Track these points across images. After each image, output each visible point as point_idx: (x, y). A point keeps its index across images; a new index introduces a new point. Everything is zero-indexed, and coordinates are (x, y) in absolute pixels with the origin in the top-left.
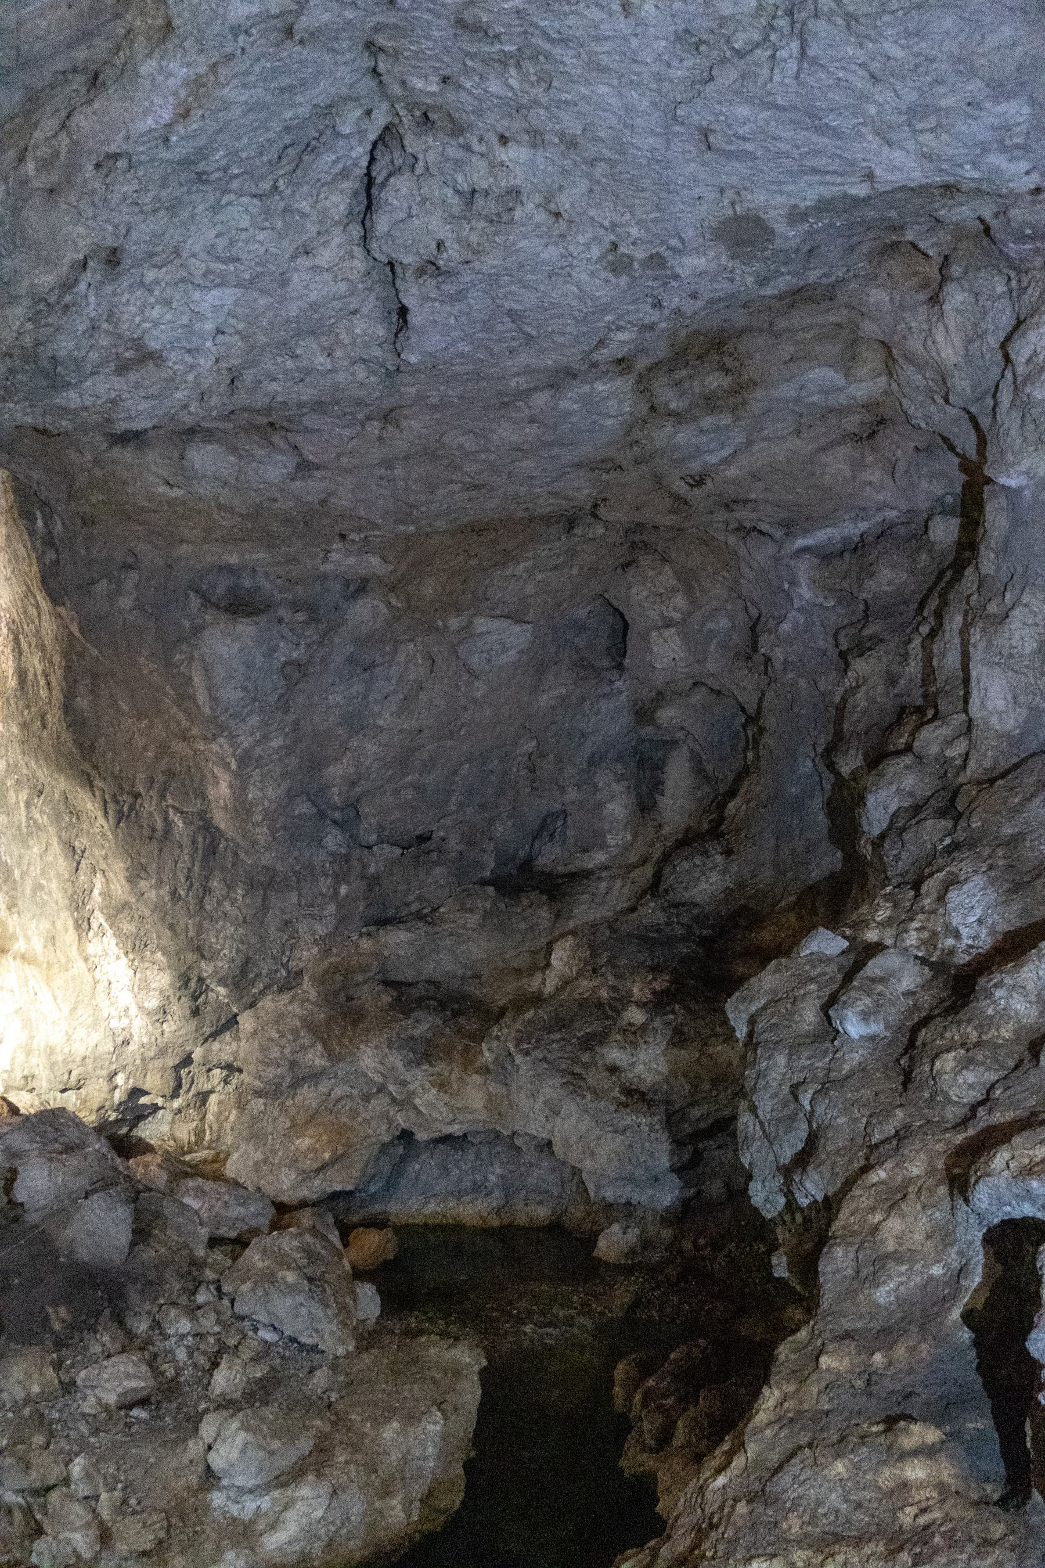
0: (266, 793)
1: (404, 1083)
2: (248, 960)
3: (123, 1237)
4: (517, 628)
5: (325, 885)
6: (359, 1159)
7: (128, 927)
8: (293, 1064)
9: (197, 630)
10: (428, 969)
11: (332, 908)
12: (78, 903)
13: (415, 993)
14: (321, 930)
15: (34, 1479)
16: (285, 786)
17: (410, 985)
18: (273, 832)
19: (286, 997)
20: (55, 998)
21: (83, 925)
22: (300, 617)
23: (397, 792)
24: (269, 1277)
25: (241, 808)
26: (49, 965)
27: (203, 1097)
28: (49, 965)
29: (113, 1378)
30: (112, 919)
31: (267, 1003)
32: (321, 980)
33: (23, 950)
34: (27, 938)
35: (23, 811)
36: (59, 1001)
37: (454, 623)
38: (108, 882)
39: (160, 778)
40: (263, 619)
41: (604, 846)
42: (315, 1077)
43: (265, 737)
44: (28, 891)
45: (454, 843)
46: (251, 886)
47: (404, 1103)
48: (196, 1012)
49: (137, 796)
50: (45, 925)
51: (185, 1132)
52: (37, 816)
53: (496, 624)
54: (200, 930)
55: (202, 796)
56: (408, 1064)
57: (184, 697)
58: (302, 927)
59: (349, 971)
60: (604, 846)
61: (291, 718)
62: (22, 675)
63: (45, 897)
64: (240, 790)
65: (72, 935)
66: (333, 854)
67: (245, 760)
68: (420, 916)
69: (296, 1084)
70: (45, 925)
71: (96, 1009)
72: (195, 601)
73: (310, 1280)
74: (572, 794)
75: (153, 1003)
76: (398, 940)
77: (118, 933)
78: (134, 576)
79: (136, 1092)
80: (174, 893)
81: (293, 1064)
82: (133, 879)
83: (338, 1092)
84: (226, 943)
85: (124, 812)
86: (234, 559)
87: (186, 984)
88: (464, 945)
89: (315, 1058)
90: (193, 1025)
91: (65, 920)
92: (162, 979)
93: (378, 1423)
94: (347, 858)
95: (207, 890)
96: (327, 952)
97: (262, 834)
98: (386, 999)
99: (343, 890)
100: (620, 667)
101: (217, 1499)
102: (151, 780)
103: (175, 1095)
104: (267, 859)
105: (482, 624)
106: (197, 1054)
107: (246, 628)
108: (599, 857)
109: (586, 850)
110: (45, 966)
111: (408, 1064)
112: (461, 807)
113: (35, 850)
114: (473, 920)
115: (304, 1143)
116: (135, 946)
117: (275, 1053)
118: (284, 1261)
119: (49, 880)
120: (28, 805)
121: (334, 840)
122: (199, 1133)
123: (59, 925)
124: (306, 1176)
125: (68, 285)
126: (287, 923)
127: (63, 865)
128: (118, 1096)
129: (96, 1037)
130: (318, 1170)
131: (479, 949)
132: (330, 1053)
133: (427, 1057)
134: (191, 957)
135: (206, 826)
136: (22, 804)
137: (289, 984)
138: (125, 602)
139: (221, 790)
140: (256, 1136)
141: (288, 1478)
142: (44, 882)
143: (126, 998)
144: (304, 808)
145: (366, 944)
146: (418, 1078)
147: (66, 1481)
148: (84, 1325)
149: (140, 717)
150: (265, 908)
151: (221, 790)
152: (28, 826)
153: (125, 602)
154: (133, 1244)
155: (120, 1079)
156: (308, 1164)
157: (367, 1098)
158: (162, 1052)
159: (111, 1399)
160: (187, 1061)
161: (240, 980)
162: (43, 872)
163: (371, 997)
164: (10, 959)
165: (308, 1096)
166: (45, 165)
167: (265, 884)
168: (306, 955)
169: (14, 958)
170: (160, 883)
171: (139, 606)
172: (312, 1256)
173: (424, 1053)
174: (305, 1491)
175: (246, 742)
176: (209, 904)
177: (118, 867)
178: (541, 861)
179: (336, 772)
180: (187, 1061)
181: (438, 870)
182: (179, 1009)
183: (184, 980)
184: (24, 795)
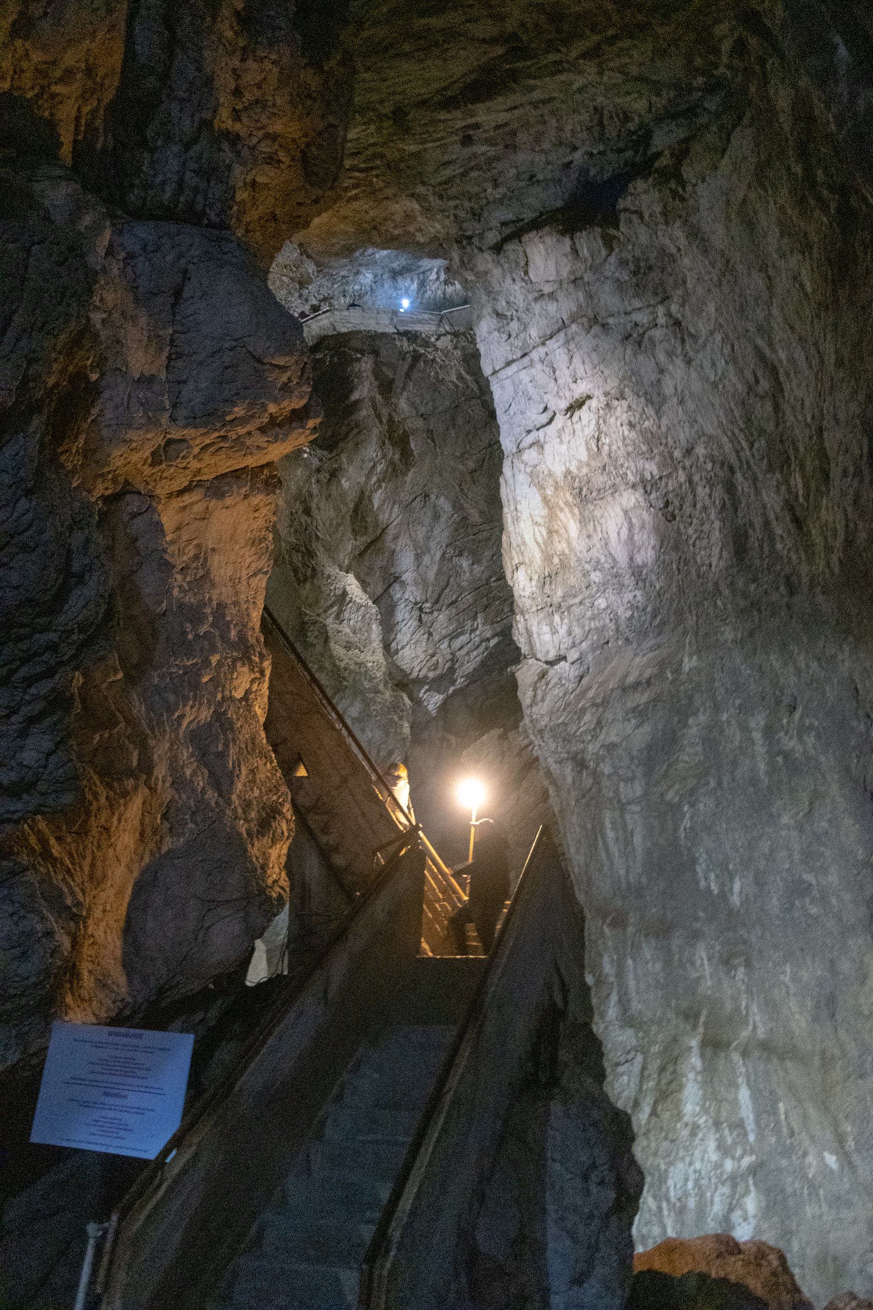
20: (841, 1139)
26: (827, 1063)
28: (827, 1063)
33: (761, 1033)
34: (772, 1008)
35: (760, 748)
36: (851, 1144)
44: (774, 903)
50: (812, 971)
52: (790, 743)
62: (739, 543)
63: (814, 910)
70: (812, 971)
110: (817, 1061)
113: (785, 820)
119: (824, 870)
120: (769, 732)
123: (845, 966)
136: (757, 736)
142: (809, 877)
152: (772, 770)
162: (808, 856)
164: (736, 1057)
169: (745, 1054)
184: (758, 722)
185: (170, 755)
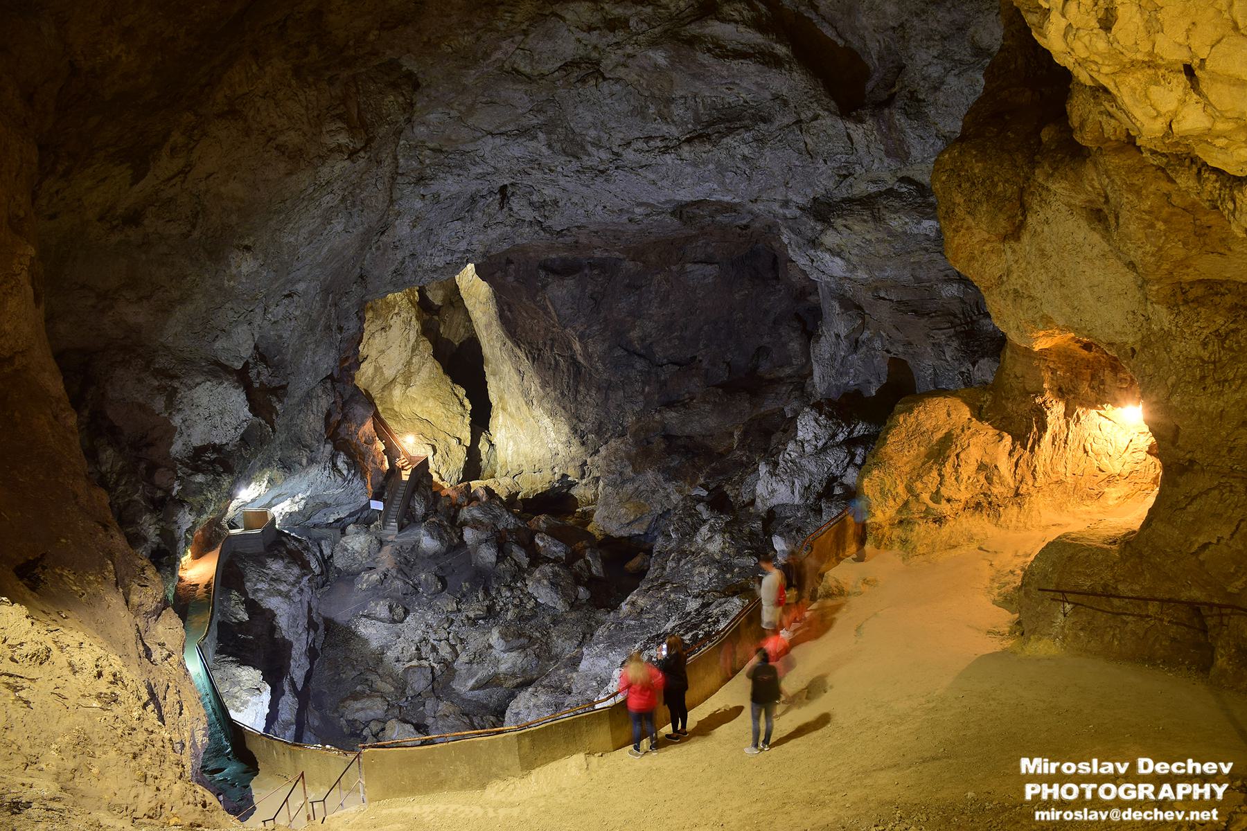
0: (597, 348)
1: (664, 489)
2: (601, 423)
3: (494, 559)
4: (710, 267)
5: (638, 386)
6: (648, 520)
7: (549, 406)
8: (621, 474)
9: (544, 287)
10: (687, 431)
11: (641, 398)
12: (525, 393)
13: (679, 442)
14: (637, 409)
15: (437, 637)
16: (606, 345)
17: (679, 437)
18: (604, 365)
19: (620, 441)
21: (529, 403)
22: (596, 272)
23: (670, 341)
24: (539, 581)
25: (588, 356)
27: (597, 479)
29: (474, 609)
30: (540, 402)
31: (612, 443)
32: (634, 435)
37: (674, 268)
38: (535, 387)
39: (549, 342)
40: (577, 276)
41: (791, 364)
42: (633, 480)
43: (590, 326)
45: (705, 364)
46: (599, 389)
47: (668, 497)
48: (583, 444)
49: (540, 350)
51: (589, 493)
53: (697, 266)
54: (577, 409)
55: (571, 349)
56: (666, 480)
57: (547, 313)
58: (627, 407)
59: (647, 431)
60: (791, 364)
61: (602, 315)
64: (585, 347)
65: (525, 408)
66: (641, 371)
67: (581, 338)
68: (684, 405)
69: (624, 482)
71: (542, 440)
72: (542, 274)
73: (552, 584)
74: (766, 339)
75: (564, 439)
76: (671, 416)
77: (544, 408)
78: (512, 266)
79: (564, 476)
80: (562, 393)
81: (621, 474)
82: (543, 387)
83: (642, 488)
84: (590, 415)
85: (536, 357)
86: (554, 256)
87: (576, 431)
88: (702, 421)
89: (629, 471)
90: (583, 449)
91: (522, 401)
92: (566, 429)
93: (558, 637)
94: (649, 373)
95: (577, 392)
96: (639, 420)
97: (600, 366)
98: (663, 446)
99: (647, 389)
100: (777, 278)
101: (494, 652)
102: (545, 344)
103: (582, 477)
104: (605, 376)
105: (689, 267)
106: (589, 460)
107: (569, 282)
108: (788, 371)
109: (781, 366)
111: (666, 480)
112: (706, 346)
114: (708, 407)
115: (623, 511)
116: (552, 414)
117: (613, 468)
118: (545, 576)
121: (640, 364)
122: (596, 496)
124: (622, 526)
125: (403, 263)
126: (619, 406)
127: (516, 378)
128: (557, 477)
129: (543, 451)
130: (628, 524)
131: (712, 422)
132: (634, 471)
133: (675, 478)
134: (575, 421)
135: (574, 362)
137: (622, 435)
138: (510, 279)
139: (577, 346)
140: (606, 504)
141: (511, 650)
143: (553, 434)
144: (619, 352)
145: (657, 417)
146: (671, 487)
147: (447, 639)
148: (473, 590)
149: (534, 319)
150: (607, 399)
151: (577, 346)
153: (510, 279)
154: (497, 563)
155: (556, 470)
156: (624, 521)
157: (653, 492)
158: (573, 459)
159: (472, 615)
160: (585, 463)
161: (599, 430)
163: (658, 444)
165: (629, 488)
166: (378, 249)
167: (606, 389)
168: (630, 420)
170: (555, 390)
171: (517, 280)
172: (555, 574)
173: (672, 475)
174: (514, 654)
175: (582, 329)
176: (580, 398)
177: (537, 381)
178: (761, 369)
179: (635, 334)
180: (585, 463)
181: (696, 379)
182: (575, 441)
183: (574, 430)
185: (370, 466)
